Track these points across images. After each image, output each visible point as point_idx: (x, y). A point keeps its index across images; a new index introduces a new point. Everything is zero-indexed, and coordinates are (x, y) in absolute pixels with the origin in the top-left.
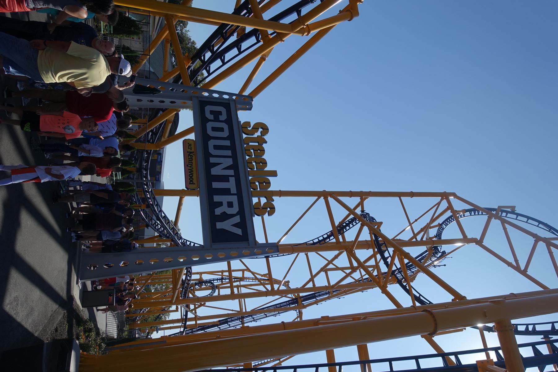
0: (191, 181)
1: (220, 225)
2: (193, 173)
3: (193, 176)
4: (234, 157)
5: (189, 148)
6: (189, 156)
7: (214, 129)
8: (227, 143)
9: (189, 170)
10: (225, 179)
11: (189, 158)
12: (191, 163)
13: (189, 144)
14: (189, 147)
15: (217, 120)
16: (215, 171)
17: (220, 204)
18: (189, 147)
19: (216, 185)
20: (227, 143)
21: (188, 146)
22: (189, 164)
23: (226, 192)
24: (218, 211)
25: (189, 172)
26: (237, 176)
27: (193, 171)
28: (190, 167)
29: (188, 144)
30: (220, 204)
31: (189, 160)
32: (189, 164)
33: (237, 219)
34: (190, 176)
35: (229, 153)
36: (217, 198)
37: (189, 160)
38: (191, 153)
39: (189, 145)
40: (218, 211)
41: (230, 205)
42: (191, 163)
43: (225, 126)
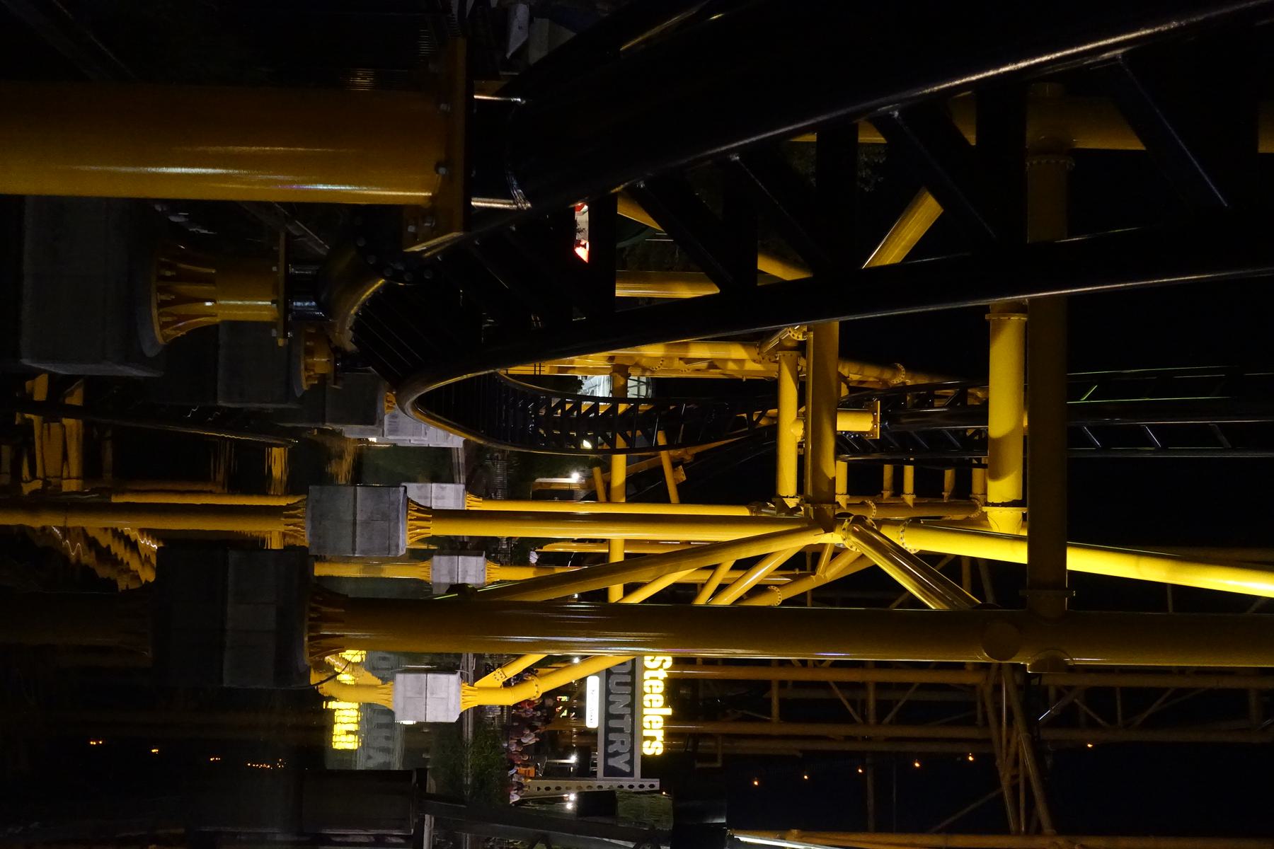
1: (611, 762)
4: (633, 694)
10: (621, 717)
16: (613, 710)
17: (613, 742)
19: (613, 724)
20: (628, 679)
23: (621, 730)
24: (611, 749)
26: (633, 715)
30: (613, 742)
33: (627, 757)
35: (628, 689)
36: (612, 737)
40: (611, 749)
41: (623, 743)
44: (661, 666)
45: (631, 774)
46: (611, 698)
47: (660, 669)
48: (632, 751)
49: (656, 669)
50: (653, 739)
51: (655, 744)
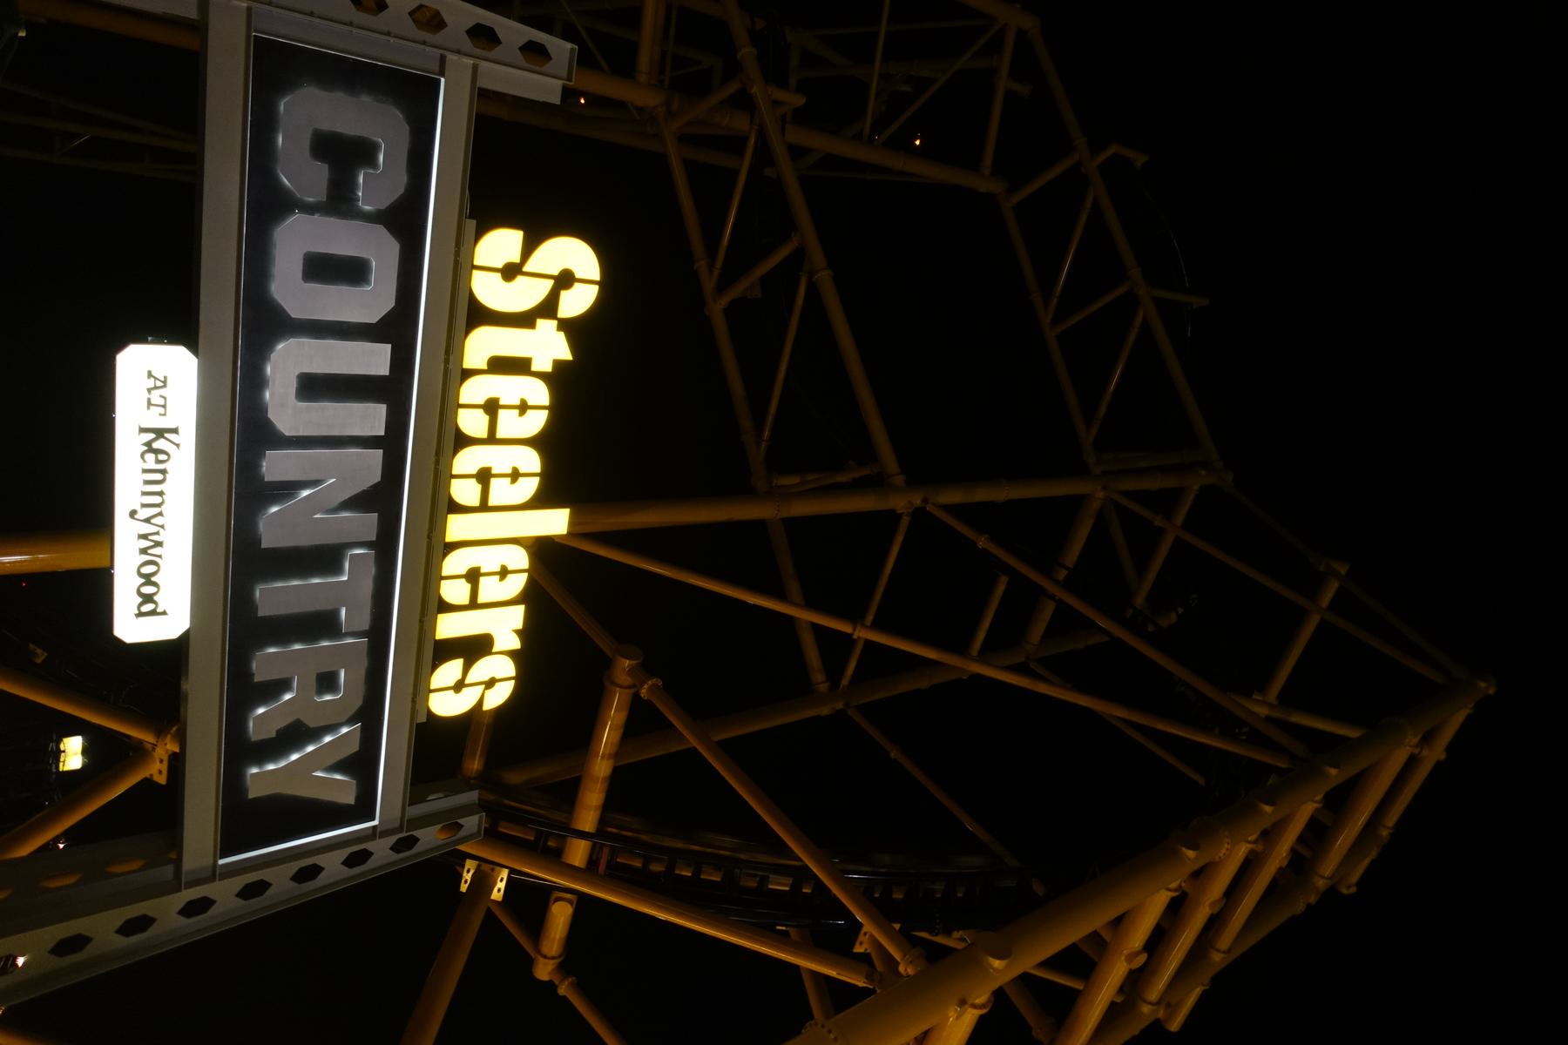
0: (148, 599)
2: (160, 556)
3: (154, 574)
4: (391, 443)
5: (149, 404)
6: (150, 457)
7: (323, 269)
8: (375, 359)
9: (144, 537)
10: (324, 558)
11: (145, 471)
12: (157, 500)
13: (156, 378)
14: (149, 400)
15: (339, 202)
18: (155, 393)
20: (375, 359)
21: (149, 390)
22: (144, 506)
23: (320, 624)
25: (144, 551)
27: (158, 544)
28: (147, 521)
29: (150, 375)
31: (147, 482)
32: (144, 506)
34: (140, 575)
35: (370, 418)
36: (269, 659)
37: (147, 482)
38: (160, 433)
39: (151, 384)
42: (157, 500)
43: (382, 253)
44: (548, 308)
45: (363, 808)
46: (276, 465)
47: (540, 322)
48: (369, 715)
49: (525, 320)
50: (474, 648)
51: (483, 668)
